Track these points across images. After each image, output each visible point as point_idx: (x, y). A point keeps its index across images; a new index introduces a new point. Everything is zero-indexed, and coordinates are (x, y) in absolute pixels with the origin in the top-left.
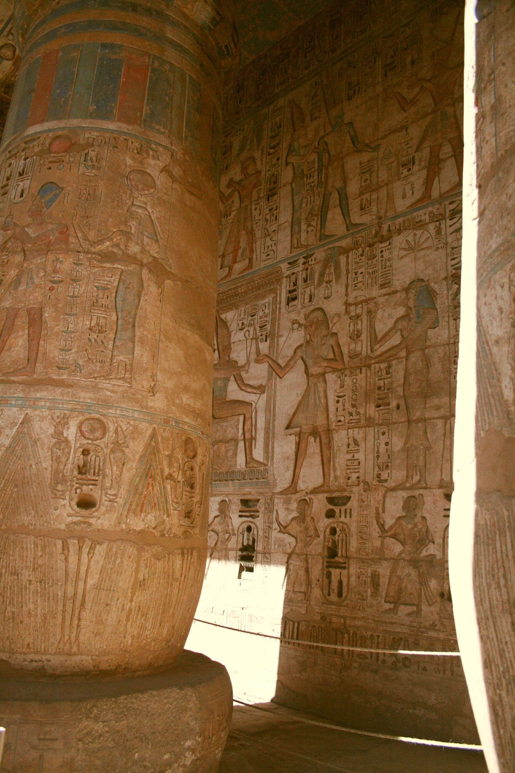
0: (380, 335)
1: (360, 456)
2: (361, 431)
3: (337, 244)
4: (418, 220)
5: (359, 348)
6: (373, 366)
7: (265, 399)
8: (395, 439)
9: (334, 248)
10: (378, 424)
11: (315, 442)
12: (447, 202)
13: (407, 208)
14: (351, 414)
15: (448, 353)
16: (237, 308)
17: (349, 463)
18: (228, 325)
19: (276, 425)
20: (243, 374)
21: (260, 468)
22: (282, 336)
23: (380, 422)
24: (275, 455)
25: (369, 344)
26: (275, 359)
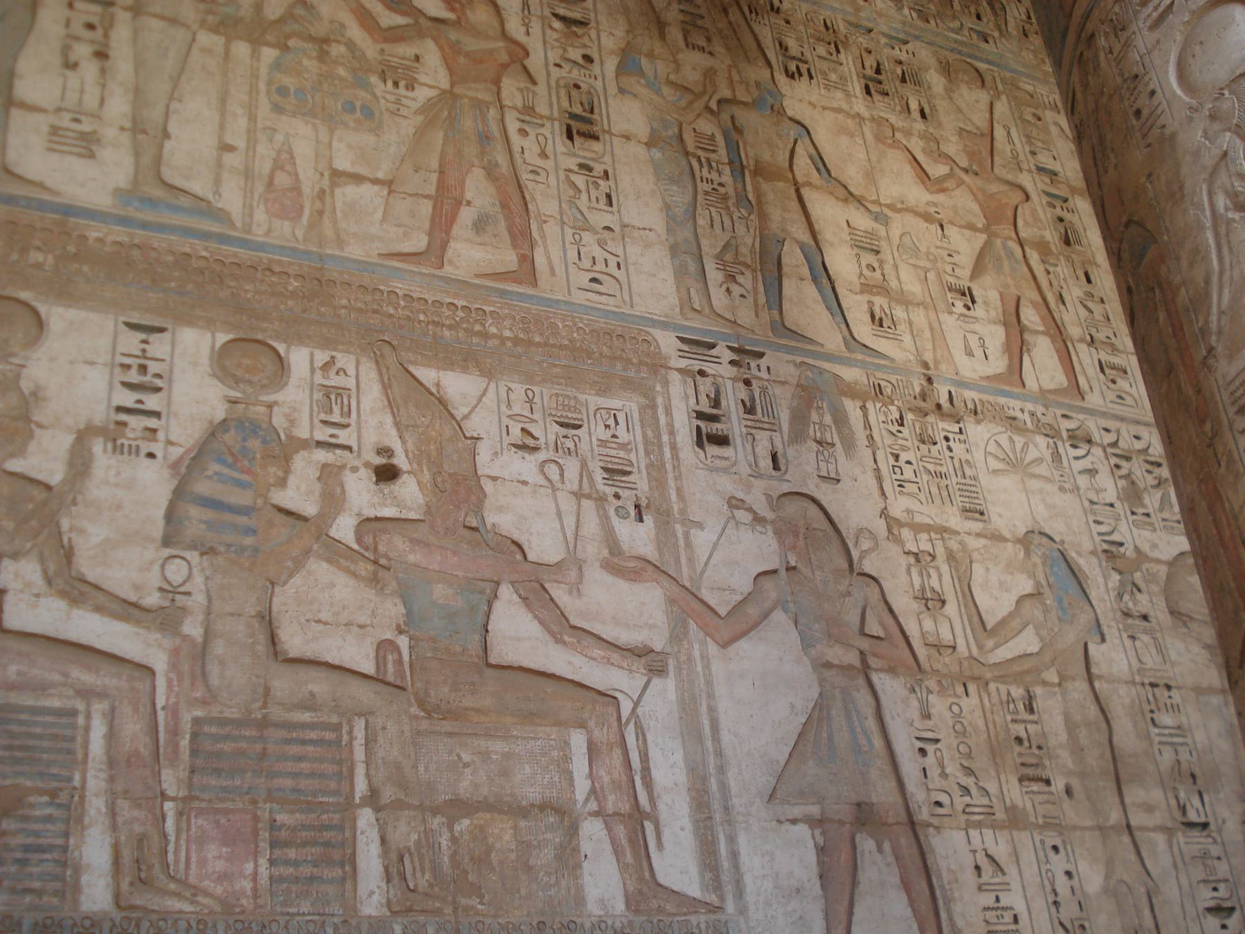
0: (990, 622)
1: (1014, 900)
2: (1003, 837)
3: (826, 365)
4: (1011, 413)
5: (946, 636)
6: (992, 686)
7: (672, 695)
8: (1084, 867)
9: (821, 371)
10: (1037, 826)
11: (880, 850)
12: (1059, 412)
13: (981, 378)
14: (966, 790)
15: (1137, 701)
16: (488, 374)
17: (991, 915)
18: (458, 414)
19: (734, 790)
20: (559, 593)
21: (693, 919)
22: (700, 526)
23: (1041, 821)
24: (748, 879)
25: (969, 631)
26: (687, 584)
